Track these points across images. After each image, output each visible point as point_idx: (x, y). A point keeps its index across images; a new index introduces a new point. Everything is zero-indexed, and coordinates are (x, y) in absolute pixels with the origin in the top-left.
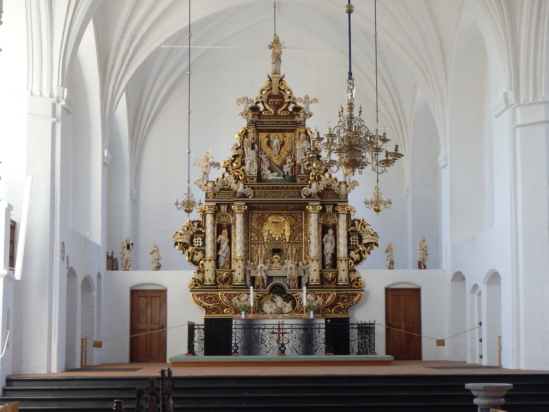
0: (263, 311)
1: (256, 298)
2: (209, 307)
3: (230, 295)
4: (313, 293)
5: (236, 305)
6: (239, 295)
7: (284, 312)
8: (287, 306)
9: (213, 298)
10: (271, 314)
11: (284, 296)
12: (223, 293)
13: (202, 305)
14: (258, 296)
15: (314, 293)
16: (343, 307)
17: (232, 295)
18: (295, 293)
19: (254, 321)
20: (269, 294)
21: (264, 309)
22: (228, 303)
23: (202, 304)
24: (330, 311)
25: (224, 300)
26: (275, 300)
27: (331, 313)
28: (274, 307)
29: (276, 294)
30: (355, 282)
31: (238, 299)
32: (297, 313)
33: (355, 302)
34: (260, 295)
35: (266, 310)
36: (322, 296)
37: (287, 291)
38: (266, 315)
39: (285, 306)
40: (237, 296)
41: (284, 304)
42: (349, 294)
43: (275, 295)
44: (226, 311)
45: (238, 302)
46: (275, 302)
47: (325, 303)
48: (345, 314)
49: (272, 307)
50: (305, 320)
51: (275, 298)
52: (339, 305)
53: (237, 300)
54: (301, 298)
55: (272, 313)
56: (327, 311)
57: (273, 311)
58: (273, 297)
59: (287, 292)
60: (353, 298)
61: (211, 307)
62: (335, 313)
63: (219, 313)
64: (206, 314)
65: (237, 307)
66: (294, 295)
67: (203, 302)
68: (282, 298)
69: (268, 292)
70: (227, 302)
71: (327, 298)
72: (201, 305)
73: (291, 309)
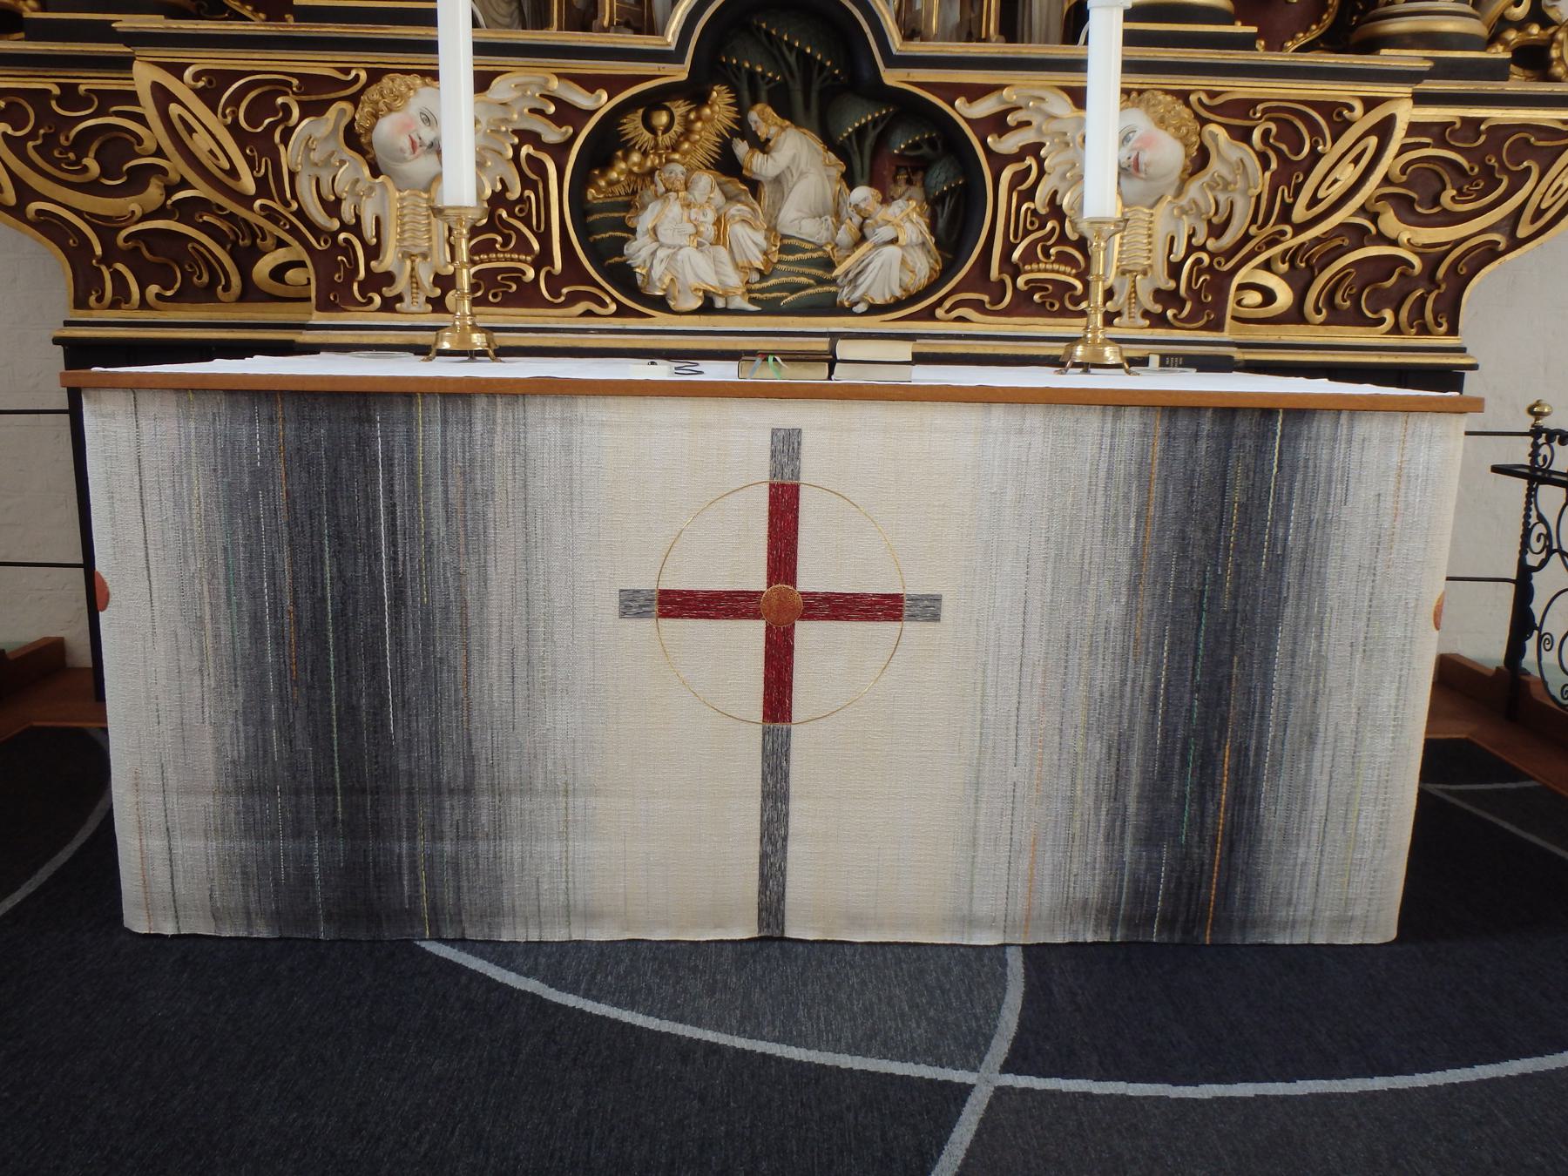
0: (624, 278)
1: (552, 135)
2: (106, 227)
3: (266, 96)
4: (1167, 92)
5: (332, 207)
6: (355, 100)
7: (844, 296)
8: (885, 233)
9: (140, 141)
10: (708, 307)
11: (858, 117)
12: (177, 70)
13: (34, 206)
14: (567, 114)
15: (1183, 96)
16: (1416, 261)
17: (281, 87)
18: (975, 93)
19: (399, 411)
20: (696, 93)
21: (638, 251)
22: (248, 184)
23: (25, 193)
24: (1285, 296)
25: (201, 143)
26: (761, 166)
27: (1296, 315)
28: (750, 241)
29: (770, 104)
30: (1520, 26)
31: (354, 139)
32: (978, 306)
33: (1539, 213)
34: (602, 102)
35: (656, 274)
36: (1266, 134)
37: (895, 61)
38: (661, 320)
39: (861, 228)
40: (338, 113)
41: (847, 211)
42: (1491, 128)
43: (762, 118)
44: (278, 273)
45: (350, 172)
46: (754, 186)
47: (1287, 210)
48: (1424, 330)
49: (719, 239)
50: (1183, 423)
51: (762, 146)
52: (1382, 239)
53: (348, 154)
54: (1034, 149)
55: (720, 303)
56: (1254, 298)
57: (734, 280)
58: (742, 129)
59: (892, 78)
60: (1519, 180)
61: (124, 233)
62: (1336, 317)
63: (207, 295)
64: (80, 303)
65: (344, 227)
66: (965, 111)
67: (35, 181)
68: (830, 142)
69: (679, 73)
70: (233, 172)
71: (1315, 157)
72: (17, 212)
73: (923, 267)
